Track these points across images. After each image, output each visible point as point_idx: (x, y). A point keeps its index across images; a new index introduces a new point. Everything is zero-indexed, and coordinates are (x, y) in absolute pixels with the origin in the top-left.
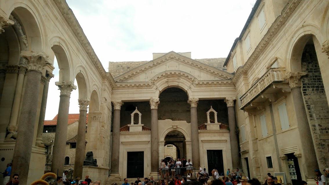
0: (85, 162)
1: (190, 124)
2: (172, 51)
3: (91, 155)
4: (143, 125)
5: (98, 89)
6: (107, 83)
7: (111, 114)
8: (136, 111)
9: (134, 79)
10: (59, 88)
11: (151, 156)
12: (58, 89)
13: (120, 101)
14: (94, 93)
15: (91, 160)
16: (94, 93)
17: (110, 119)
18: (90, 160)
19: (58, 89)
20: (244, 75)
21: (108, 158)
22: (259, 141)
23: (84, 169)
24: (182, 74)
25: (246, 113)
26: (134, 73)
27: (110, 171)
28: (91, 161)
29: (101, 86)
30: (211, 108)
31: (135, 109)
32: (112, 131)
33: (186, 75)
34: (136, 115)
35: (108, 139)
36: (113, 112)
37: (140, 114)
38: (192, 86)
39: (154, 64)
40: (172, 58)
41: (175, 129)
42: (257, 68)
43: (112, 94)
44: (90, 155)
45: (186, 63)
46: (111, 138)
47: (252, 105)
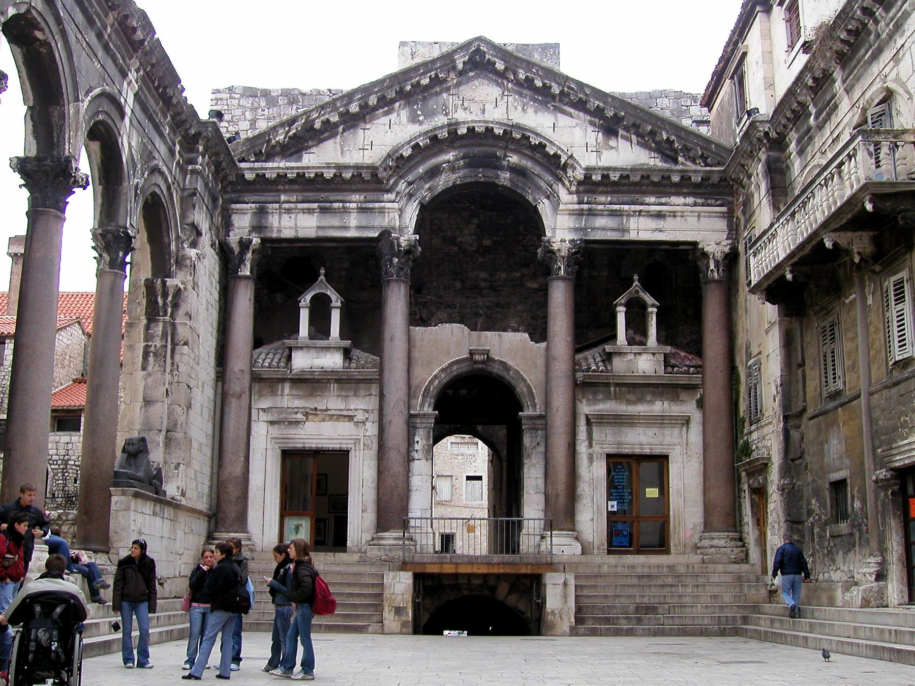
0: (117, 474)
1: (543, 345)
2: (479, 39)
3: (141, 451)
4: (347, 343)
5: (169, 188)
8: (323, 287)
9: (313, 150)
10: (23, 182)
11: (380, 472)
12: (20, 186)
15: (143, 468)
18: (137, 468)
19: (20, 186)
20: (769, 149)
21: (207, 470)
22: (811, 419)
23: (114, 499)
25: (771, 311)
26: (317, 125)
27: (213, 521)
28: (141, 474)
29: (179, 177)
30: (636, 283)
31: (314, 278)
37: (336, 300)
39: (402, 89)
41: (480, 366)
42: (820, 127)
44: (136, 450)
45: (536, 90)
46: (219, 391)
47: (789, 277)
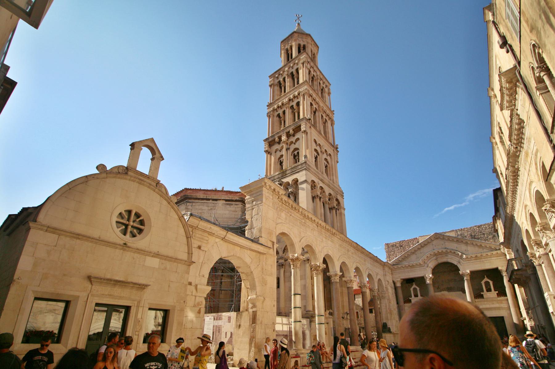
6: (387, 269)
7: (394, 290)
13: (399, 280)
14: (379, 280)
16: (379, 280)
17: (394, 294)
24: (448, 251)
32: (397, 303)
33: (453, 252)
34: (415, 289)
35: (395, 312)
36: (396, 288)
37: (418, 289)
38: (461, 260)
40: (437, 238)
43: (392, 274)
